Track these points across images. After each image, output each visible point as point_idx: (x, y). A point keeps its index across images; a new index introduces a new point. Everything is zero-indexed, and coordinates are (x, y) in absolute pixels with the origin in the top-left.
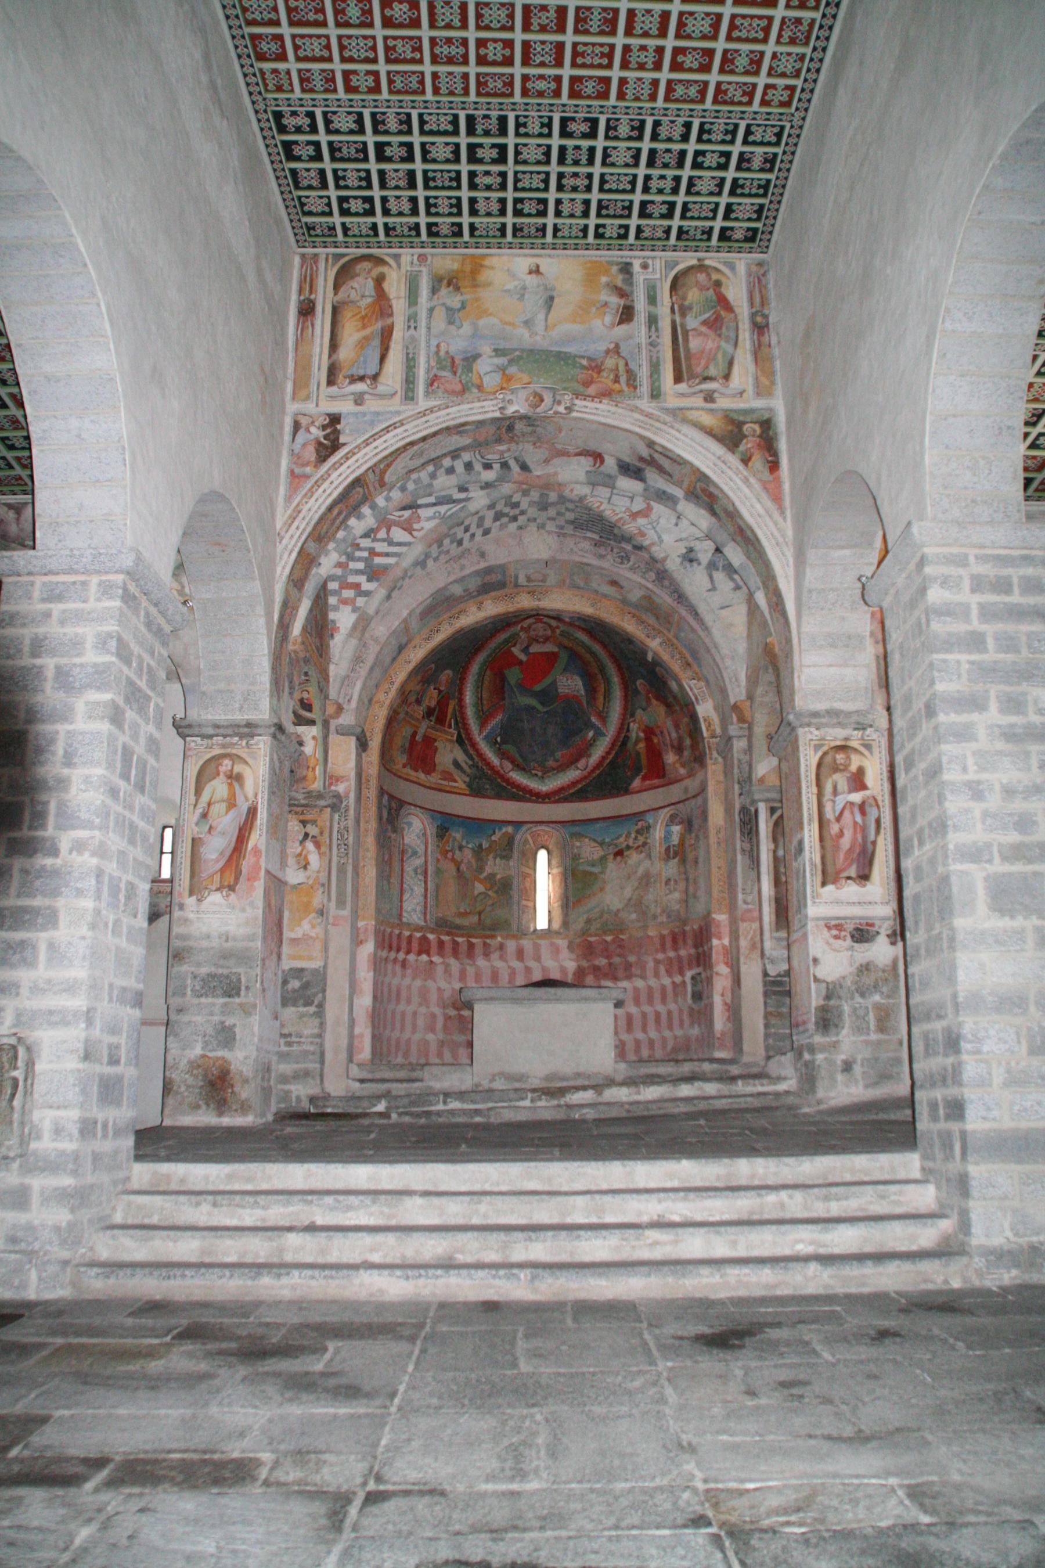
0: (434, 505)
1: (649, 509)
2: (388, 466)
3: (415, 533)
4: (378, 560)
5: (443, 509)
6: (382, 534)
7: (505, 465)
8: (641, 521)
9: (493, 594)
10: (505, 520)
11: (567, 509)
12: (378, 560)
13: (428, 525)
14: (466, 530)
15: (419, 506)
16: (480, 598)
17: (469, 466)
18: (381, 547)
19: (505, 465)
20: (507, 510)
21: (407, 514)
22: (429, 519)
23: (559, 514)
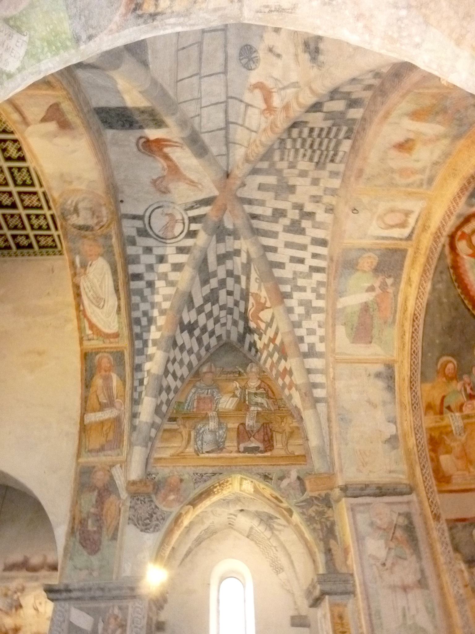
0: (248, 278)
1: (260, 86)
2: (92, 326)
3: (268, 304)
4: (278, 342)
5: (254, 275)
6: (263, 326)
7: (193, 220)
8: (276, 101)
9: (407, 262)
10: (305, 224)
11: (292, 166)
12: (278, 342)
13: (263, 293)
14: (301, 261)
15: (248, 289)
16: (404, 276)
17: (181, 250)
18: (270, 333)
19: (193, 220)
20: (286, 221)
21: (251, 300)
22: (260, 288)
23: (303, 174)
